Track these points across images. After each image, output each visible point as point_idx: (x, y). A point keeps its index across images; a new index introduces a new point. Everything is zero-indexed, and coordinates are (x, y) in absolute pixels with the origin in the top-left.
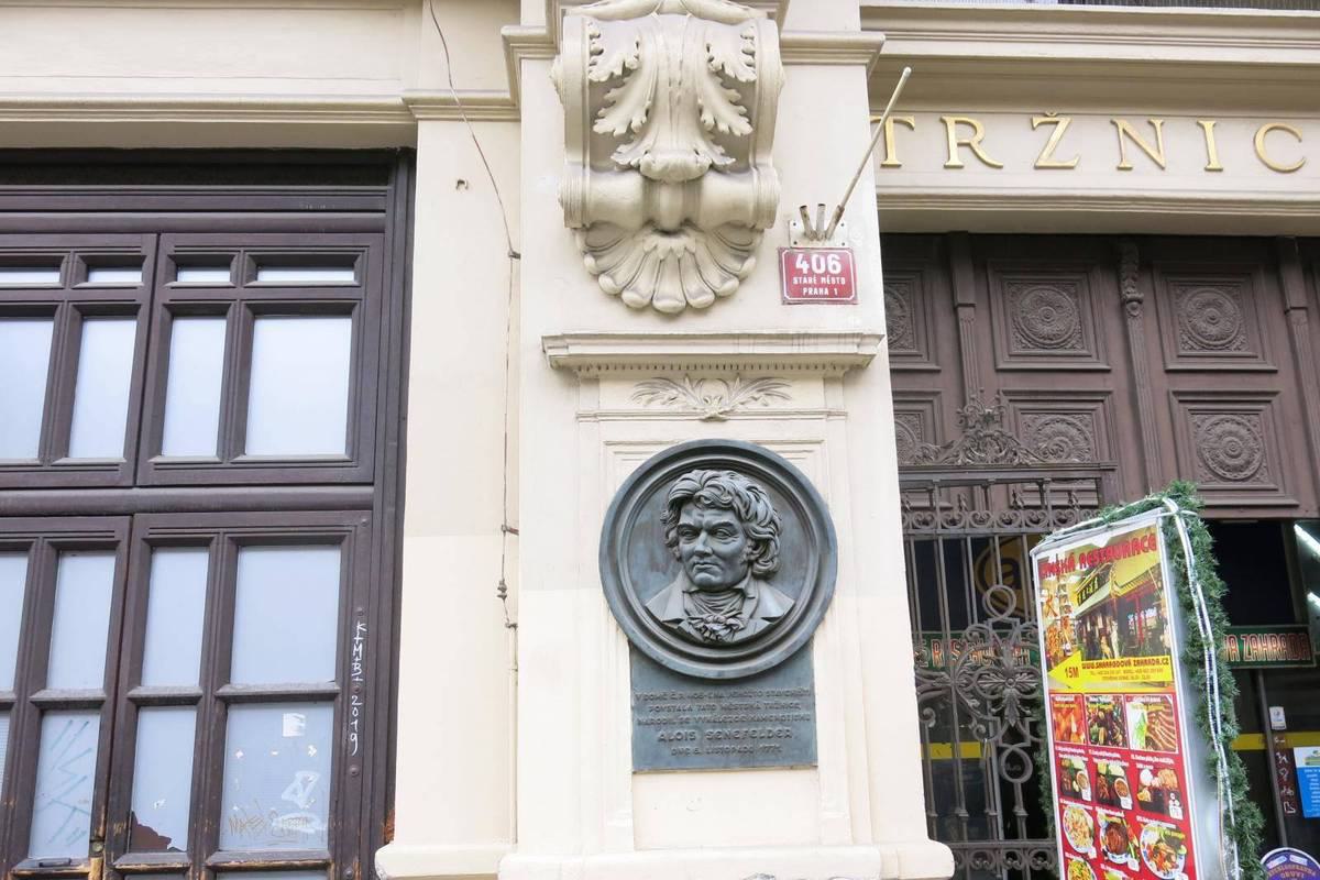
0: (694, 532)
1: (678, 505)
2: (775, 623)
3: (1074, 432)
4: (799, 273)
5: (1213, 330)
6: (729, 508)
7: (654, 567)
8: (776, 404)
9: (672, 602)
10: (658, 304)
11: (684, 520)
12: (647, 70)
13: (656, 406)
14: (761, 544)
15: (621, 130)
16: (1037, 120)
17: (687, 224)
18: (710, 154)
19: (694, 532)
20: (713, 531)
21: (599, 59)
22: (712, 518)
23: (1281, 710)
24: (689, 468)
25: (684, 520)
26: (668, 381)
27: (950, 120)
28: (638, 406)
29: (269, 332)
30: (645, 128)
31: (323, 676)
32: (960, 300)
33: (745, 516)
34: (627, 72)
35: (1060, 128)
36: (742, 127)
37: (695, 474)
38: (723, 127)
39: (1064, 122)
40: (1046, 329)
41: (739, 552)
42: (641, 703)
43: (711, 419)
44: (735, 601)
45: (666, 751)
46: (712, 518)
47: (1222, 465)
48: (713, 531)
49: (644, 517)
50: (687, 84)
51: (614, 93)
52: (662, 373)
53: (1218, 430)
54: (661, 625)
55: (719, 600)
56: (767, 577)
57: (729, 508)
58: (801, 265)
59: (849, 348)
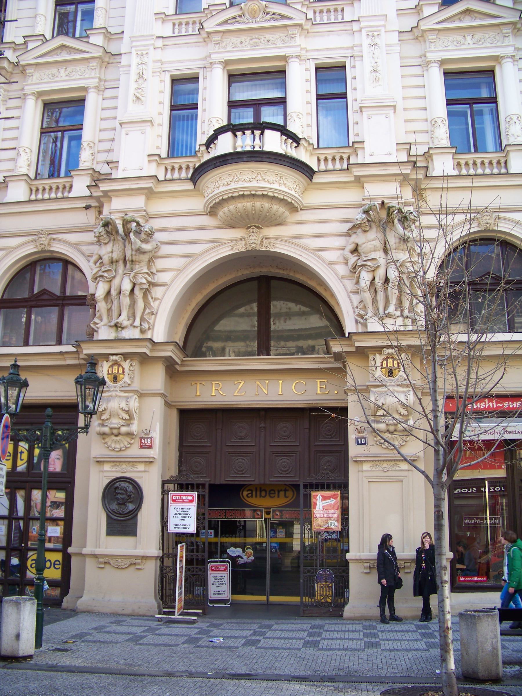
0: (118, 494)
2: (132, 511)
3: (243, 461)
4: (142, 443)
6: (123, 490)
8: (135, 469)
10: (116, 450)
14: (129, 497)
15: (106, 419)
17: (119, 434)
18: (122, 422)
19: (118, 494)
20: (121, 494)
27: (214, 383)
30: (110, 418)
33: (126, 491)
36: (128, 417)
38: (124, 418)
40: (241, 434)
47: (281, 470)
48: (121, 494)
51: (103, 412)
52: (116, 463)
53: (281, 461)
54: (112, 510)
55: (122, 506)
56: (131, 502)
57: (123, 490)
58: (143, 441)
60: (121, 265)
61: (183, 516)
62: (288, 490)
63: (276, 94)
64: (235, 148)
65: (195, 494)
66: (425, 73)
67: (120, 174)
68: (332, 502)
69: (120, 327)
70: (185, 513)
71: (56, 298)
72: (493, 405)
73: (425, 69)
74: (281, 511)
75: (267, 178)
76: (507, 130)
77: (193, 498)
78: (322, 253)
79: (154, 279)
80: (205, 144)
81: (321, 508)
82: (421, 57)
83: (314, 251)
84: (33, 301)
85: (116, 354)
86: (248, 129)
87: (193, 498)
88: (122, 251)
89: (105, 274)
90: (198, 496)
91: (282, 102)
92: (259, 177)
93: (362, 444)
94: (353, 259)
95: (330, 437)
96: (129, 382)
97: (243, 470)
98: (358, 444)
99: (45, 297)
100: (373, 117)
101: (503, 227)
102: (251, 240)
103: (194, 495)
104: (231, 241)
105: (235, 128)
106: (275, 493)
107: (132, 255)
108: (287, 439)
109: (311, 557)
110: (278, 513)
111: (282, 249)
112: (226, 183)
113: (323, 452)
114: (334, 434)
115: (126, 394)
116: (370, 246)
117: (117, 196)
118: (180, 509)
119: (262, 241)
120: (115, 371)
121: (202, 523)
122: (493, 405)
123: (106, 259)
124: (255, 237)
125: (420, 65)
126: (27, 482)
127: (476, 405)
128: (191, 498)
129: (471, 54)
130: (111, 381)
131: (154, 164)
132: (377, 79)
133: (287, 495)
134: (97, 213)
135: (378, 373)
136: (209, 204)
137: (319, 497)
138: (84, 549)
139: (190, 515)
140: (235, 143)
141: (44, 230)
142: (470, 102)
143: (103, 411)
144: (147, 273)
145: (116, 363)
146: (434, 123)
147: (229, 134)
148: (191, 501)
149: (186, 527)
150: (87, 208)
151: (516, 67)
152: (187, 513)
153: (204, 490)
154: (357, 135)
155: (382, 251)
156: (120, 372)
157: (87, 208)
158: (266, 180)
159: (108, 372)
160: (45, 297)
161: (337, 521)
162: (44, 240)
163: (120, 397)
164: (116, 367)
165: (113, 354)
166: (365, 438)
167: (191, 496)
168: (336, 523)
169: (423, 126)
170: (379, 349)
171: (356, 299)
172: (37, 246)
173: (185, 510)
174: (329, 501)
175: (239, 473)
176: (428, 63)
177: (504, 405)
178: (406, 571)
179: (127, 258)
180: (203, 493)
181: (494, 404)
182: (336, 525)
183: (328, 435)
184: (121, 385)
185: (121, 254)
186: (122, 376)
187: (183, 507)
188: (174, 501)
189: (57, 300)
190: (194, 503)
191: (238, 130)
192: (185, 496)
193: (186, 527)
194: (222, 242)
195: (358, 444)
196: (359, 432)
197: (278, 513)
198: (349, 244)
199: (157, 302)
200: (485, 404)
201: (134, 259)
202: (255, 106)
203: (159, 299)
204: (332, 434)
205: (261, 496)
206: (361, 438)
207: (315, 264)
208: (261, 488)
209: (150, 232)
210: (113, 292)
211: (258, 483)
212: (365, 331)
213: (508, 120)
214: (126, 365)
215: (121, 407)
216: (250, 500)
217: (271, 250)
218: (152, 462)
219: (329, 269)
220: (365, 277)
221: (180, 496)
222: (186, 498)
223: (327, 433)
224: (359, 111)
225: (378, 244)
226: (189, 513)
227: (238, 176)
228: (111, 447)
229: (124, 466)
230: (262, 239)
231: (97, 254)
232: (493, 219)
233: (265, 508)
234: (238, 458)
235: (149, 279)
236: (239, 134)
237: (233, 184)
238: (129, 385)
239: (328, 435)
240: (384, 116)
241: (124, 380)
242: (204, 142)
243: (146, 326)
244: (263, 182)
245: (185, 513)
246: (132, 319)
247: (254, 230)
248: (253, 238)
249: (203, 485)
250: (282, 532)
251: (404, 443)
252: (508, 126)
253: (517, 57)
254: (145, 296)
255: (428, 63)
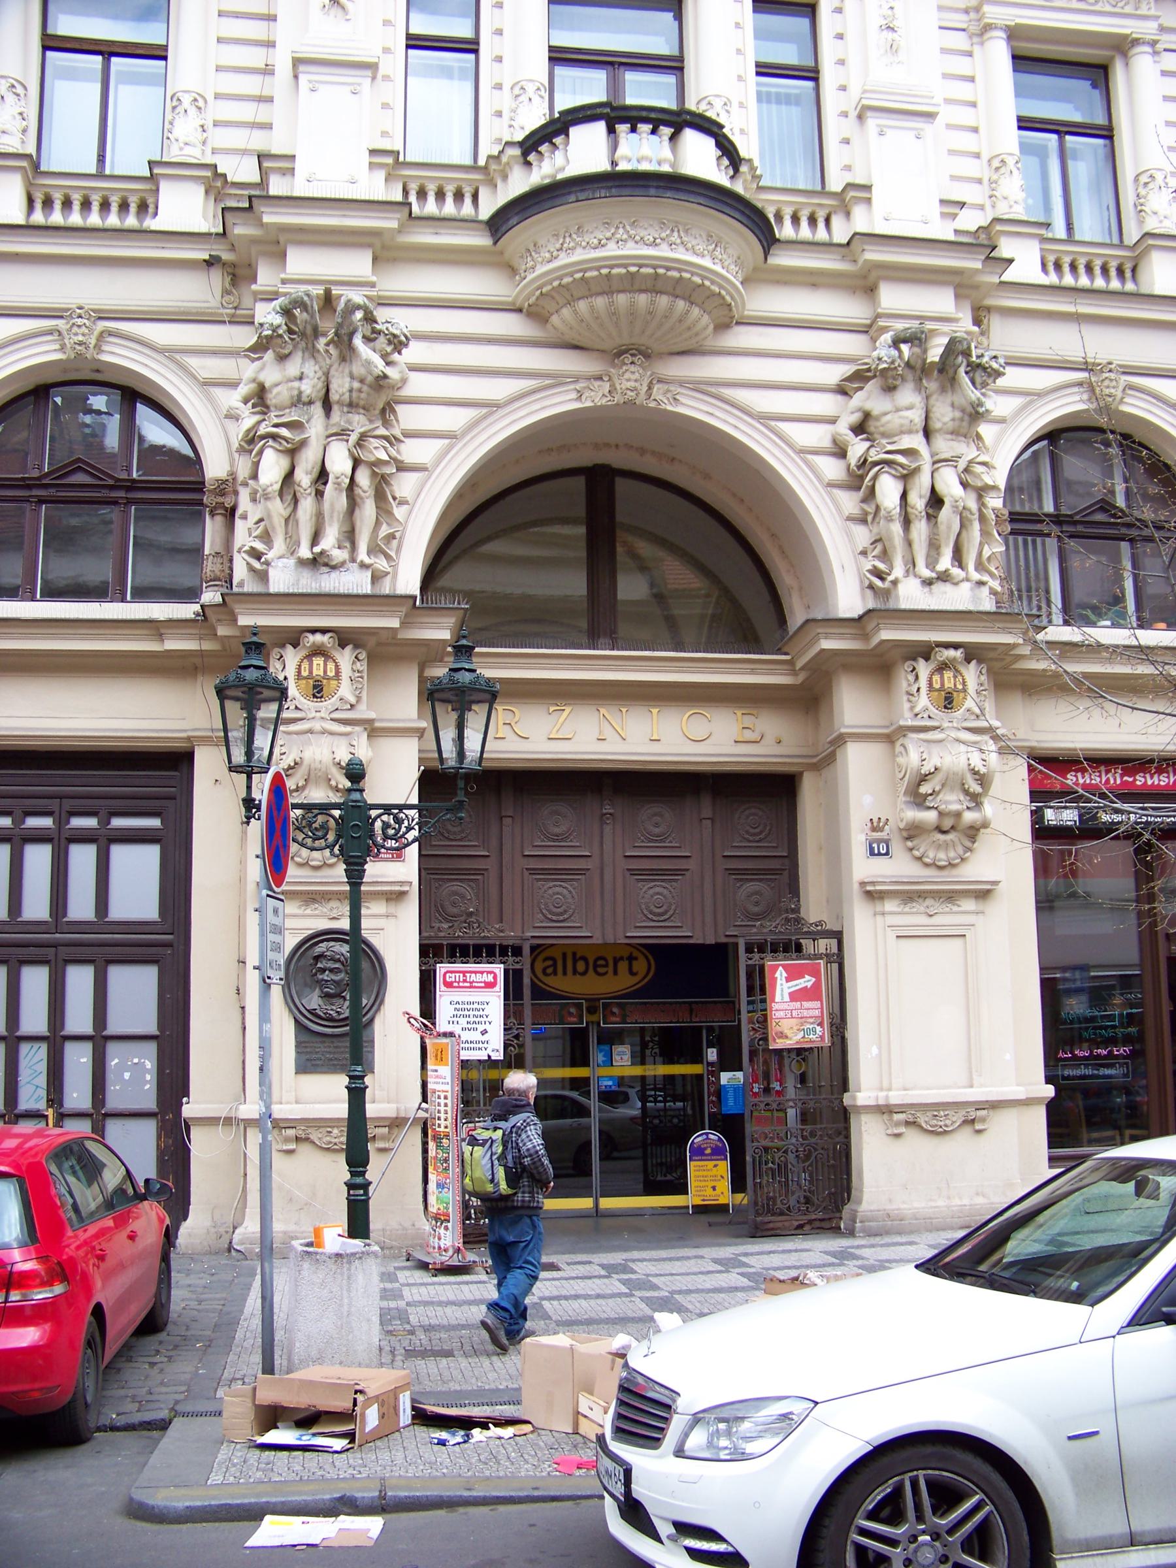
0: (323, 970)
1: (317, 958)
3: (565, 891)
5: (657, 830)
6: (338, 960)
7: (306, 985)
9: (314, 1001)
10: (311, 863)
11: (319, 965)
12: (306, 763)
13: (308, 911)
16: (552, 709)
19: (323, 970)
20: (331, 970)
21: (284, 757)
22: (331, 965)
23: (715, 1050)
24: (322, 941)
25: (319, 965)
26: (314, 900)
28: (300, 912)
29: (119, 853)
30: (304, 787)
31: (152, 1028)
32: (503, 814)
34: (296, 764)
35: (565, 714)
37: (324, 944)
38: (340, 786)
39: (568, 709)
40: (557, 830)
41: (342, 980)
42: (298, 1045)
43: (334, 918)
44: (341, 1001)
45: (309, 1064)
46: (331, 965)
47: (651, 912)
48: (331, 970)
49: (301, 963)
50: (324, 769)
53: (651, 892)
55: (334, 1000)
57: (338, 960)
59: (397, 888)
60: (317, 410)
61: (472, 1019)
62: (636, 959)
63: (659, 45)
64: (614, 163)
65: (499, 969)
66: (976, 50)
67: (300, 188)
68: (809, 984)
69: (326, 565)
70: (476, 1013)
71: (111, 482)
72: (1115, 778)
73: (975, 40)
74: (619, 1005)
75: (691, 241)
76: (1142, 201)
77: (495, 977)
78: (786, 427)
79: (398, 452)
80: (521, 144)
81: (787, 998)
82: (966, 11)
83: (765, 419)
84: (46, 486)
85: (323, 631)
86: (645, 120)
87: (495, 977)
88: (323, 378)
89: (284, 432)
90: (506, 971)
91: (674, 65)
92: (675, 238)
93: (879, 854)
94: (857, 448)
95: (757, 838)
96: (353, 700)
97: (565, 911)
98: (872, 853)
99: (80, 478)
100: (889, 132)
101: (1135, 407)
102: (628, 380)
103: (497, 971)
104: (577, 379)
105: (613, 115)
106: (606, 966)
107: (351, 391)
108: (661, 841)
109: (767, 1104)
110: (615, 1010)
111: (692, 408)
112: (596, 241)
113: (745, 871)
114: (767, 831)
115: (348, 729)
116: (903, 421)
117: (300, 243)
118: (463, 1003)
119: (650, 388)
120: (318, 671)
121: (517, 1037)
122: (1115, 780)
123: (279, 395)
124: (637, 376)
125: (964, 30)
126: (55, 945)
127: (1152, 778)
128: (490, 978)
129: (1073, 22)
130: (306, 696)
131: (381, 175)
132: (893, 48)
133: (635, 970)
134: (228, 279)
135: (923, 701)
136: (540, 287)
137: (781, 974)
138: (242, 1107)
139: (489, 1019)
140: (614, 147)
141: (86, 307)
142: (1060, 129)
143: (290, 768)
144: (385, 438)
145: (318, 651)
146: (999, 164)
147: (599, 128)
148: (490, 985)
149: (481, 1045)
150: (211, 263)
151: (1159, 67)
152: (481, 1013)
153: (517, 959)
154: (848, 168)
155: (921, 434)
156: (331, 674)
157: (211, 263)
158: (689, 245)
159: (299, 672)
160: (80, 478)
161: (821, 1024)
162: (84, 334)
163: (332, 733)
164: (318, 661)
165: (314, 631)
166: (887, 842)
167: (488, 972)
168: (819, 1029)
169: (972, 168)
170: (925, 651)
171: (862, 535)
172: (63, 348)
173: (476, 1006)
174: (802, 981)
175: (554, 918)
176: (988, 28)
177: (1135, 780)
178: (978, 1126)
179: (334, 397)
180: (518, 966)
181: (1118, 776)
182: (818, 1035)
183: (754, 834)
184: (332, 705)
185: (320, 385)
186: (334, 682)
187: (472, 999)
188: (448, 985)
189: (112, 488)
190: (497, 988)
191: (623, 120)
192: (475, 972)
193: (481, 1045)
194: (556, 380)
195: (872, 853)
196: (874, 829)
197: (615, 1010)
198: (847, 412)
199: (405, 508)
200: (1100, 776)
201: (355, 400)
202: (610, 68)
203: (406, 503)
204: (761, 833)
205: (575, 972)
206: (879, 841)
207: (769, 450)
208: (574, 954)
209: (403, 338)
210: (304, 478)
211: (600, 942)
212: (883, 607)
213: (1144, 179)
214: (345, 658)
215: (337, 760)
216: (550, 980)
217: (669, 408)
218: (988, 892)
219: (801, 463)
220: (888, 490)
221: (464, 973)
222: (479, 978)
223: (748, 828)
224: (853, 114)
225: (917, 416)
226: (486, 1012)
227: (628, 228)
228: (300, 856)
229: (929, 902)
230: (651, 382)
231: (254, 380)
232: (1121, 388)
233: (586, 1000)
234: (552, 884)
235: (393, 453)
236: (622, 128)
237: (612, 245)
238: (352, 706)
239: (754, 834)
240: (912, 134)
241: (339, 694)
242: (520, 136)
243: (381, 564)
244: (681, 249)
245: (476, 1013)
246: (348, 545)
247: (635, 359)
248: (633, 377)
249: (517, 951)
250: (624, 1053)
251: (968, 854)
252: (1142, 192)
253: (1159, 47)
254: (380, 496)
255: (988, 28)
